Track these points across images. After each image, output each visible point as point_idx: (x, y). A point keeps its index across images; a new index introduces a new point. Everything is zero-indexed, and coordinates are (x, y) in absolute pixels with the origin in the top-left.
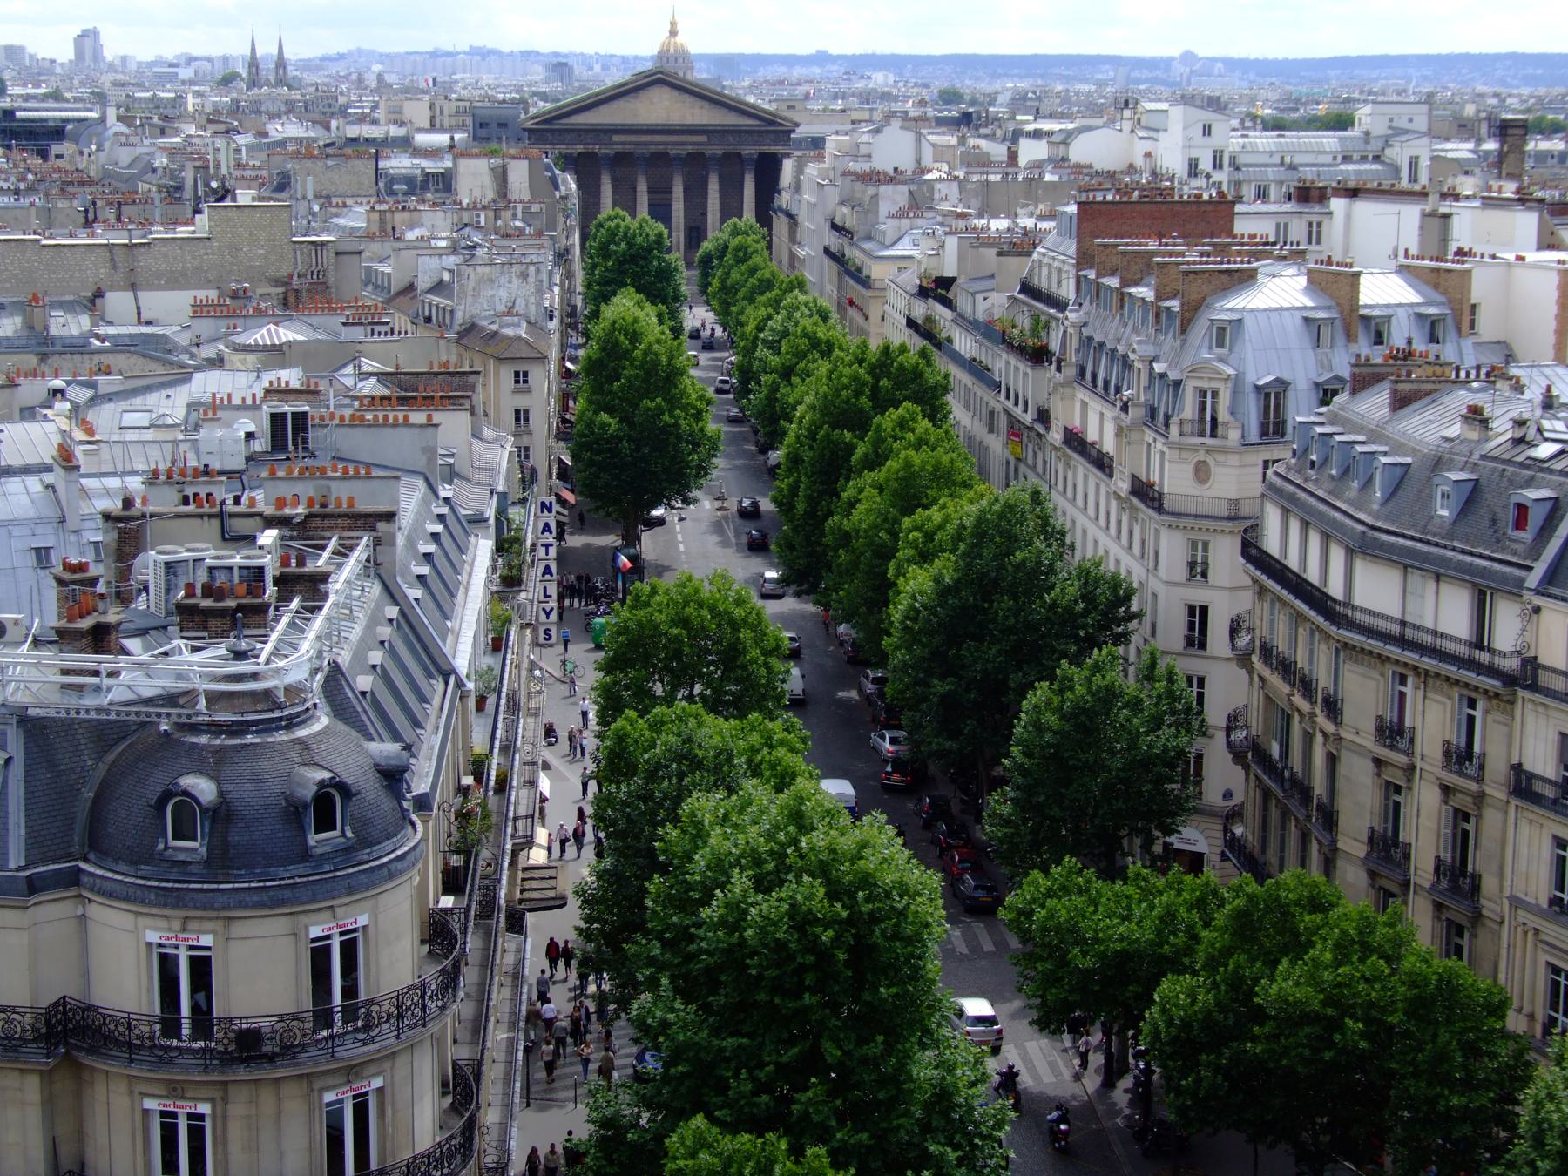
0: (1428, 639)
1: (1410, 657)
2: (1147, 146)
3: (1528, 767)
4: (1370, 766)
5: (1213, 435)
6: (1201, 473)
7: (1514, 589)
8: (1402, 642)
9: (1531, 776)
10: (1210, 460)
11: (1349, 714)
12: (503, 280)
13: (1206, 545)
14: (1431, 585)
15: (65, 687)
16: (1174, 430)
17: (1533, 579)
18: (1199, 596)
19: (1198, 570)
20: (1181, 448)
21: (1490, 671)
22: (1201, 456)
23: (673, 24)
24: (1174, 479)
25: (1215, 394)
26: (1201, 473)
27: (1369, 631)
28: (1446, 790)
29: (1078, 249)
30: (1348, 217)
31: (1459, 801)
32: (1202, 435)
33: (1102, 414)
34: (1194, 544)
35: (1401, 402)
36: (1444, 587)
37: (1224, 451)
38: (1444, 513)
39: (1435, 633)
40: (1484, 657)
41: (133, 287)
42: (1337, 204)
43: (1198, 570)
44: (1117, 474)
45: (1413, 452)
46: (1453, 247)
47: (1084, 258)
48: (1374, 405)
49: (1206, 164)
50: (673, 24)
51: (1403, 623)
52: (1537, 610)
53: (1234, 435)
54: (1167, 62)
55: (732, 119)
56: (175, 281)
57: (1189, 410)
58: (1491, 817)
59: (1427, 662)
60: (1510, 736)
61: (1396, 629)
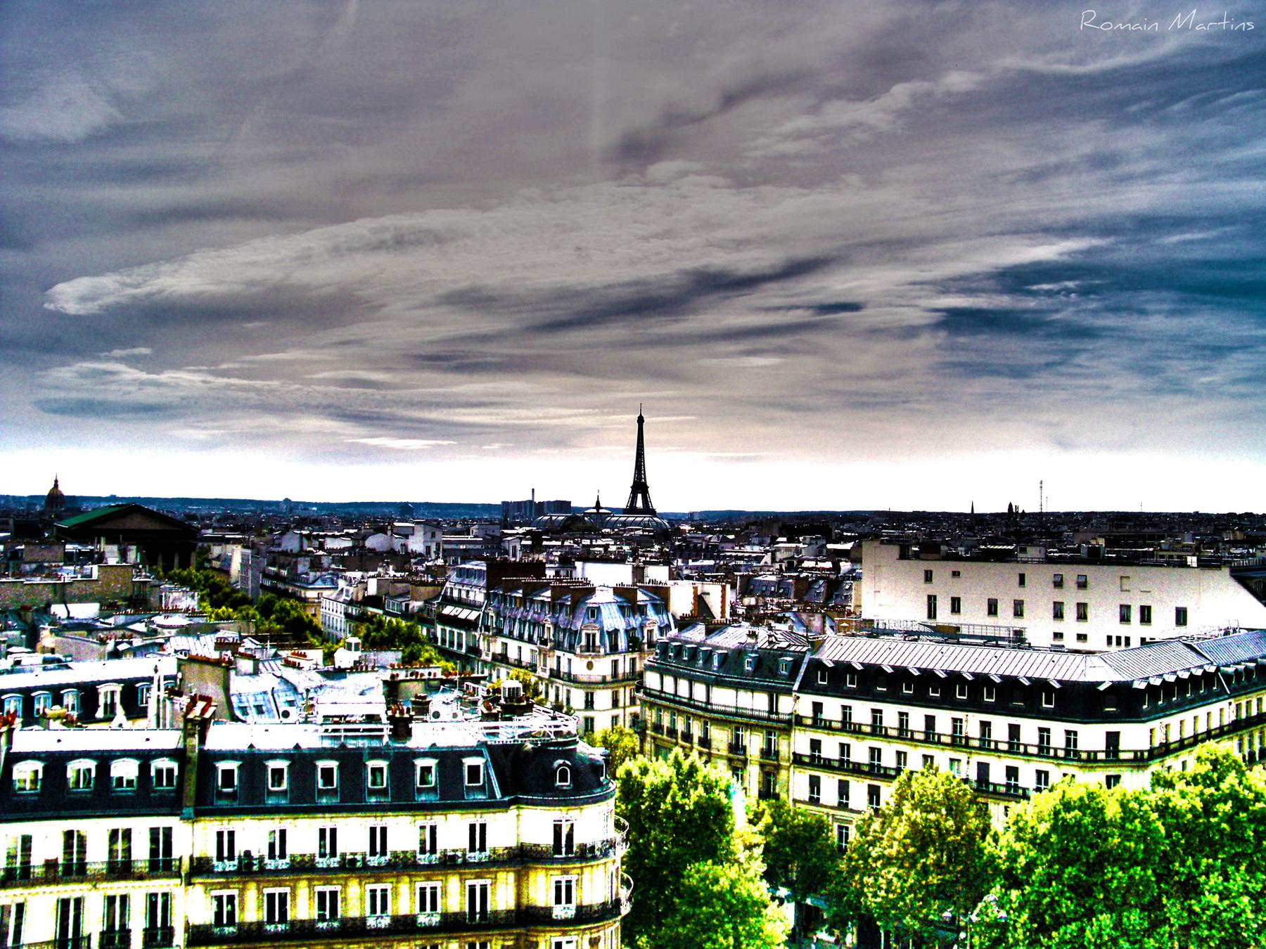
0: (749, 712)
1: (739, 719)
2: (403, 541)
3: (797, 752)
4: (725, 762)
5: (593, 651)
6: (590, 666)
7: (788, 692)
8: (736, 714)
9: (801, 756)
10: (593, 661)
11: (714, 744)
12: (184, 599)
13: (592, 694)
14: (750, 694)
15: (488, 734)
16: (578, 651)
17: (796, 687)
18: (589, 714)
19: (589, 704)
20: (581, 656)
21: (778, 721)
22: (590, 659)
23: (56, 481)
24: (578, 667)
25: (594, 635)
26: (590, 666)
27: (724, 713)
28: (762, 766)
29: (487, 582)
30: (583, 569)
31: (767, 769)
32: (588, 651)
33: (520, 648)
34: (587, 694)
35: (709, 632)
36: (755, 694)
37: (598, 656)
38: (750, 668)
39: (752, 710)
40: (774, 716)
41: (65, 603)
42: (578, 564)
43: (589, 704)
44: (539, 670)
45: (726, 648)
46: (647, 580)
47: (489, 587)
48: (697, 634)
49: (433, 548)
50: (56, 481)
51: (737, 708)
52: (798, 698)
53: (602, 650)
54: (277, 503)
55: (154, 526)
56: (82, 599)
57: (584, 643)
58: (783, 774)
59: (753, 721)
60: (789, 744)
61: (734, 710)
